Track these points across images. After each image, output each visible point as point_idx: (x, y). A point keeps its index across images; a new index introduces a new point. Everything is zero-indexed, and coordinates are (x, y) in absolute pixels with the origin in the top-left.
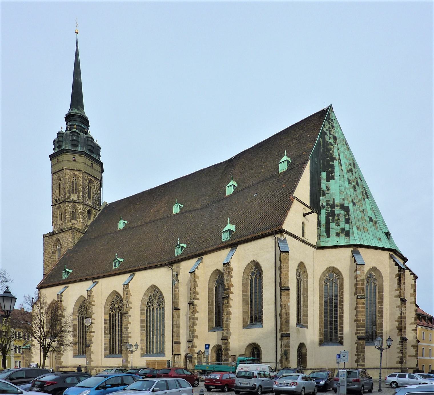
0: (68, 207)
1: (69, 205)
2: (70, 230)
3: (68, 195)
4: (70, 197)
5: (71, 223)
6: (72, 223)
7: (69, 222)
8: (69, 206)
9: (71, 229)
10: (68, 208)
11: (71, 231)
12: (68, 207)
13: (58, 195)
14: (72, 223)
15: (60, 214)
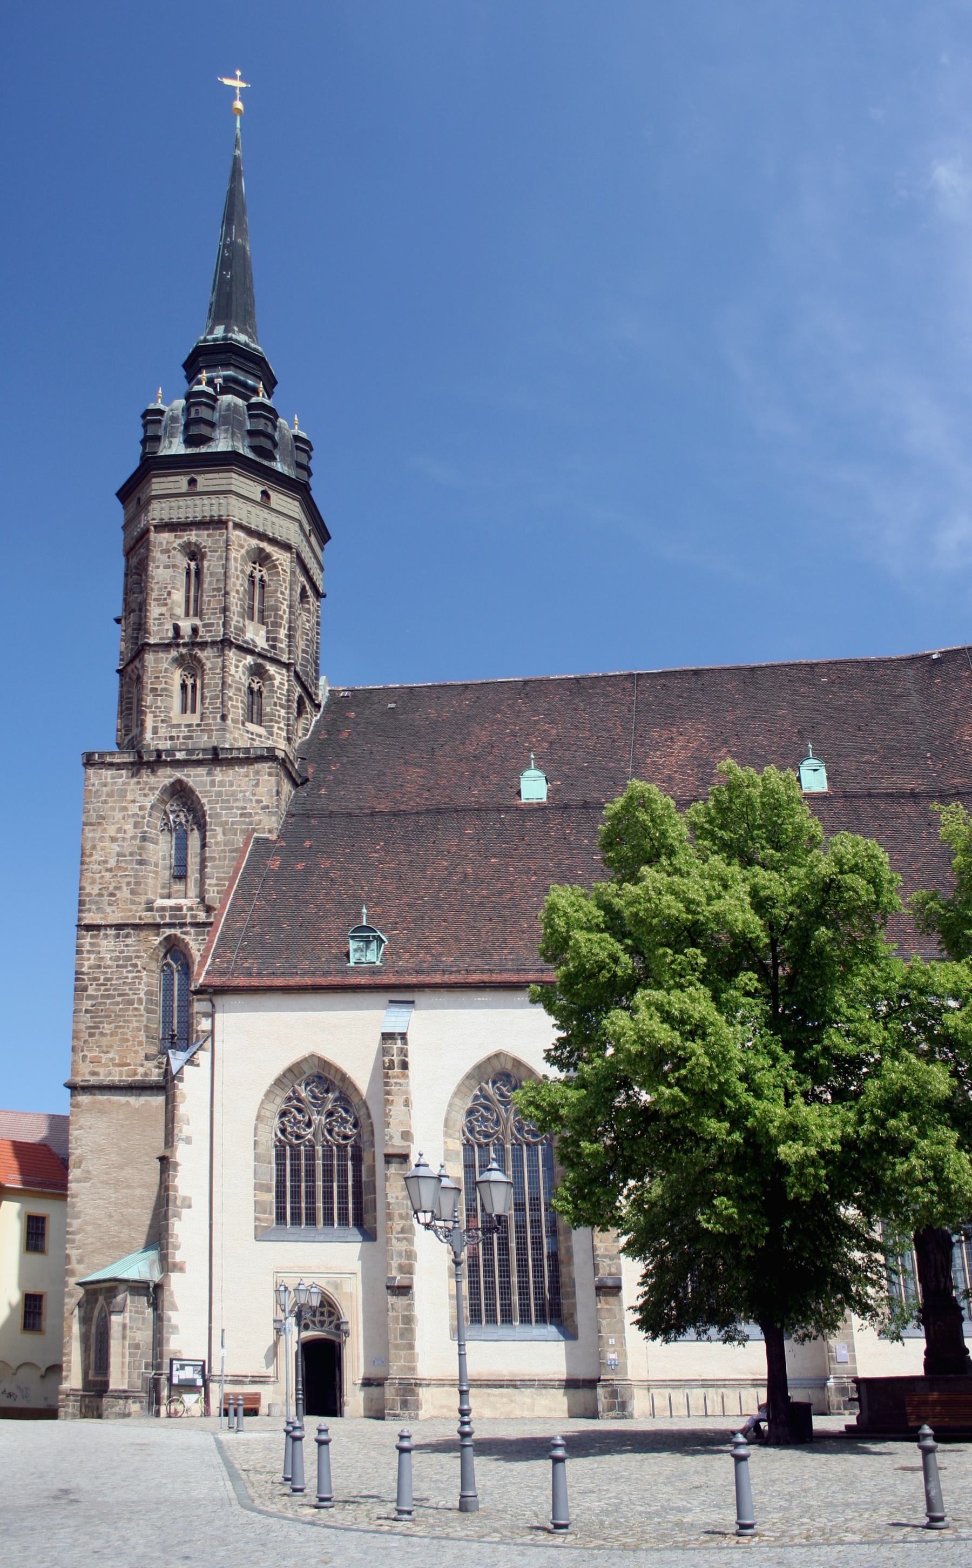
0: (237, 667)
1: (240, 661)
2: (260, 759)
3: (237, 622)
4: (242, 630)
5: (248, 732)
6: (252, 734)
7: (240, 726)
8: (241, 664)
9: (274, 758)
10: (237, 672)
11: (266, 765)
12: (237, 667)
13: (180, 611)
14: (252, 734)
15: (184, 686)
